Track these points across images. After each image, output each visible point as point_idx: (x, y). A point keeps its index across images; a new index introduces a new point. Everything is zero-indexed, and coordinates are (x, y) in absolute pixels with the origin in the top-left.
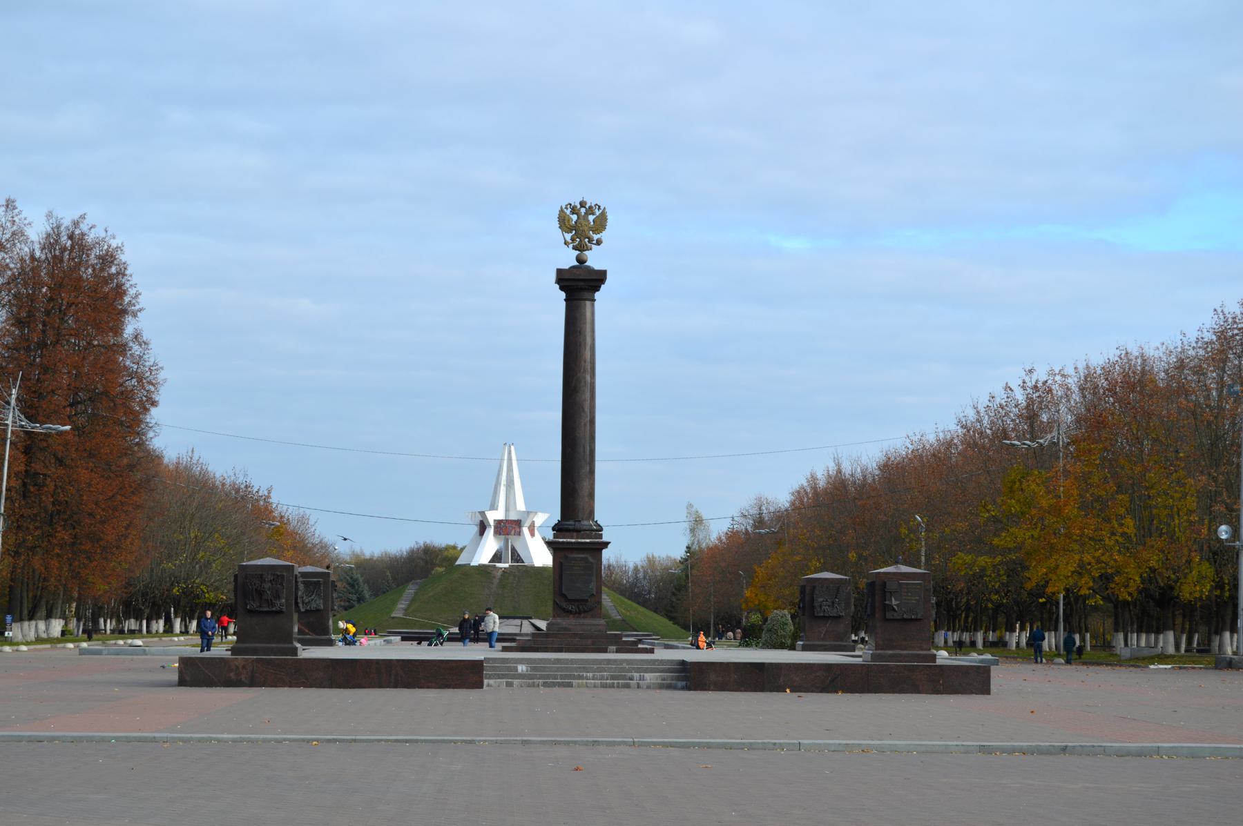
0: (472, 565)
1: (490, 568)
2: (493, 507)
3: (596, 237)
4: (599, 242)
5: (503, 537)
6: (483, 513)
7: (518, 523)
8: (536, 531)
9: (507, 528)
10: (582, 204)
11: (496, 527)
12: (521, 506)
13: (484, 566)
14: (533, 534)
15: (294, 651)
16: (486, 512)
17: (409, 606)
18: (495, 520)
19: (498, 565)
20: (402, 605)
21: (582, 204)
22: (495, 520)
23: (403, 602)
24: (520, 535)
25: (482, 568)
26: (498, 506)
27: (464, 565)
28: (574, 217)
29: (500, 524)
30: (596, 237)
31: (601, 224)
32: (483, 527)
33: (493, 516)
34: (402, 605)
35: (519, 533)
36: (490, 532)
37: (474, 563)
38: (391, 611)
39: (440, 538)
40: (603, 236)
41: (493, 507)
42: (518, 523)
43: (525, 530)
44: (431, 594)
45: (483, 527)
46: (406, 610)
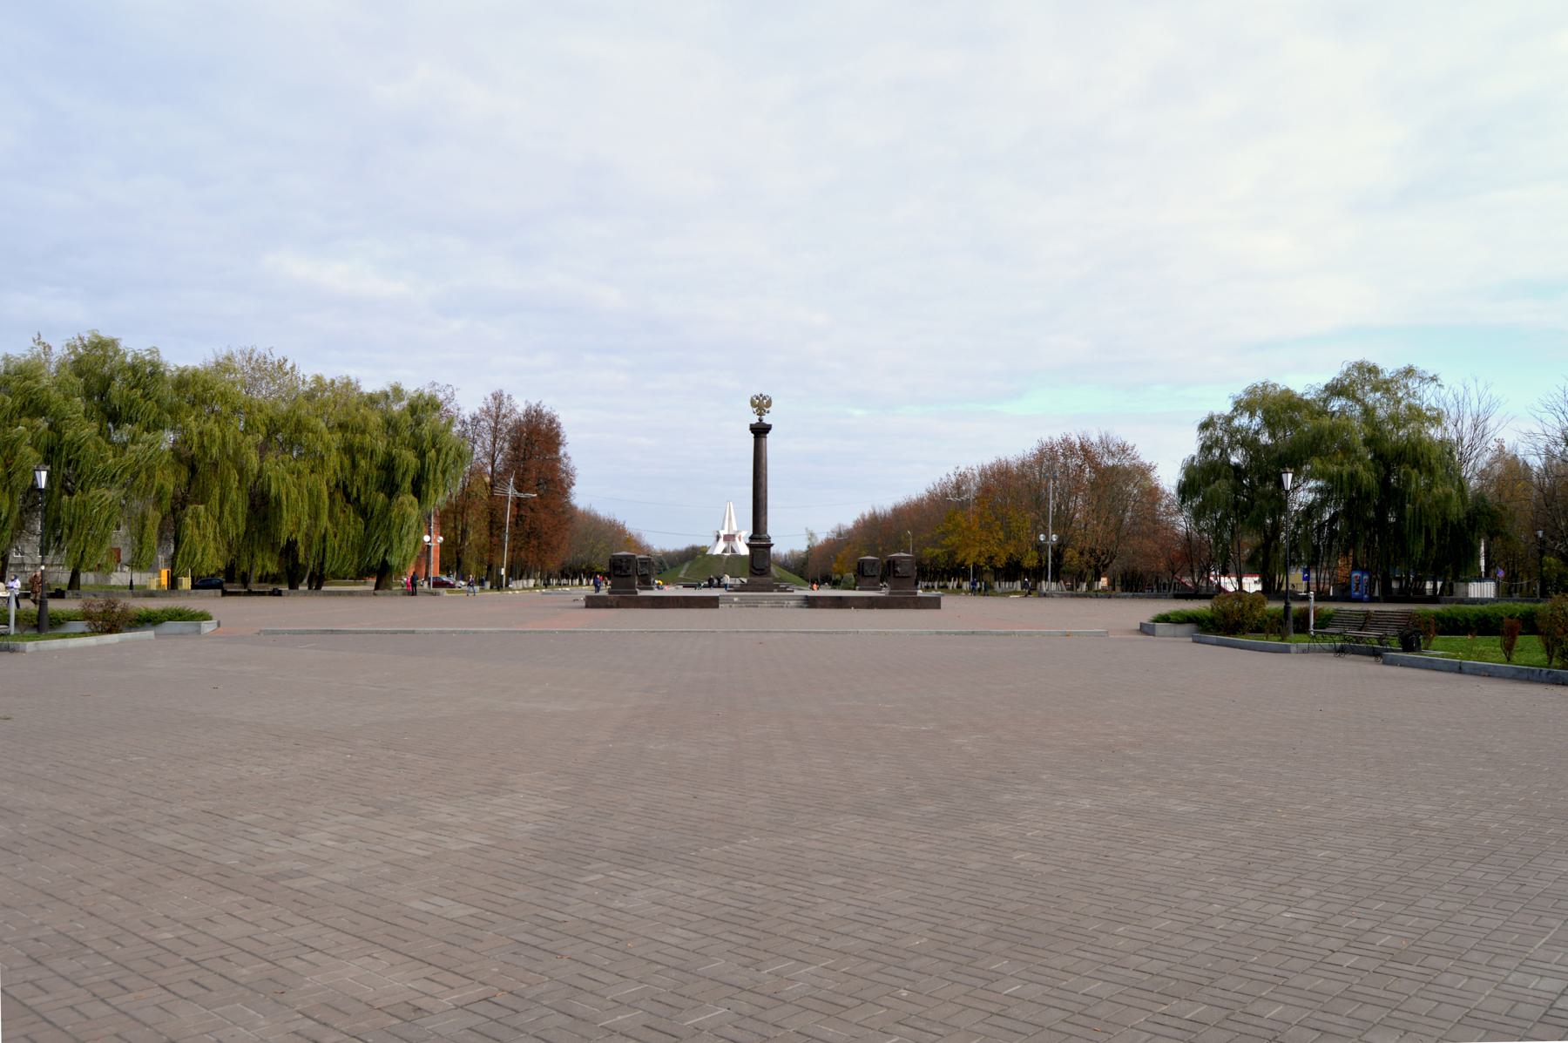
2: (723, 529)
3: (767, 410)
4: (768, 412)
6: (718, 532)
7: (734, 536)
9: (729, 538)
10: (761, 395)
12: (735, 528)
13: (718, 555)
15: (636, 593)
21: (761, 395)
25: (718, 556)
28: (758, 401)
30: (767, 410)
31: (769, 404)
32: (718, 538)
33: (722, 533)
35: (734, 540)
36: (721, 540)
37: (715, 553)
39: (699, 543)
40: (770, 409)
41: (723, 529)
42: (734, 536)
43: (737, 539)
45: (718, 538)
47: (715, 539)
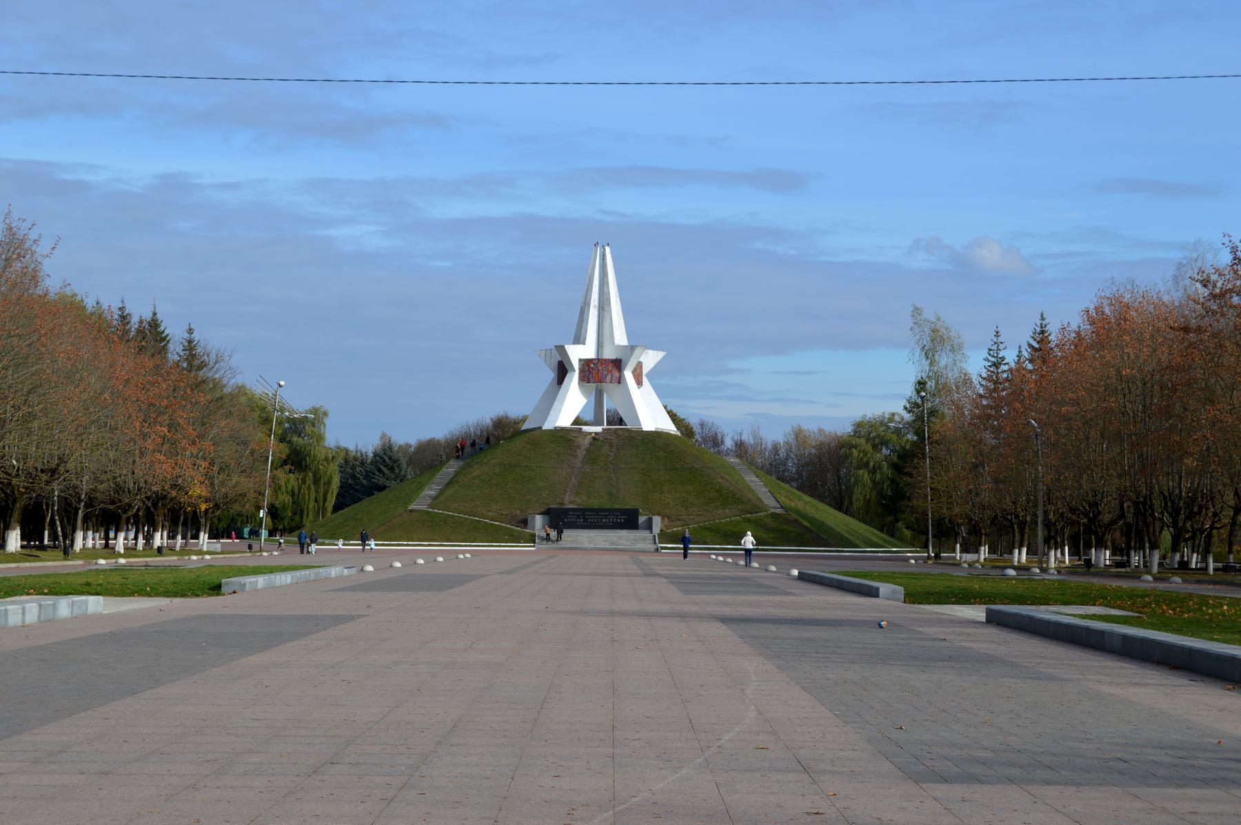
0: (544, 428)
1: (571, 433)
2: (579, 339)
5: (593, 386)
6: (561, 349)
7: (618, 364)
8: (645, 380)
11: (582, 371)
13: (563, 429)
14: (639, 383)
16: (566, 347)
17: (441, 492)
18: (580, 360)
19: (585, 428)
20: (430, 491)
22: (580, 360)
23: (434, 486)
24: (619, 382)
25: (560, 432)
26: (585, 338)
27: (534, 429)
29: (589, 366)
32: (562, 370)
33: (578, 354)
34: (430, 491)
36: (573, 380)
37: (547, 426)
38: (410, 501)
41: (579, 339)
42: (618, 364)
43: (628, 374)
44: (477, 473)
46: (435, 498)
47: (551, 375)
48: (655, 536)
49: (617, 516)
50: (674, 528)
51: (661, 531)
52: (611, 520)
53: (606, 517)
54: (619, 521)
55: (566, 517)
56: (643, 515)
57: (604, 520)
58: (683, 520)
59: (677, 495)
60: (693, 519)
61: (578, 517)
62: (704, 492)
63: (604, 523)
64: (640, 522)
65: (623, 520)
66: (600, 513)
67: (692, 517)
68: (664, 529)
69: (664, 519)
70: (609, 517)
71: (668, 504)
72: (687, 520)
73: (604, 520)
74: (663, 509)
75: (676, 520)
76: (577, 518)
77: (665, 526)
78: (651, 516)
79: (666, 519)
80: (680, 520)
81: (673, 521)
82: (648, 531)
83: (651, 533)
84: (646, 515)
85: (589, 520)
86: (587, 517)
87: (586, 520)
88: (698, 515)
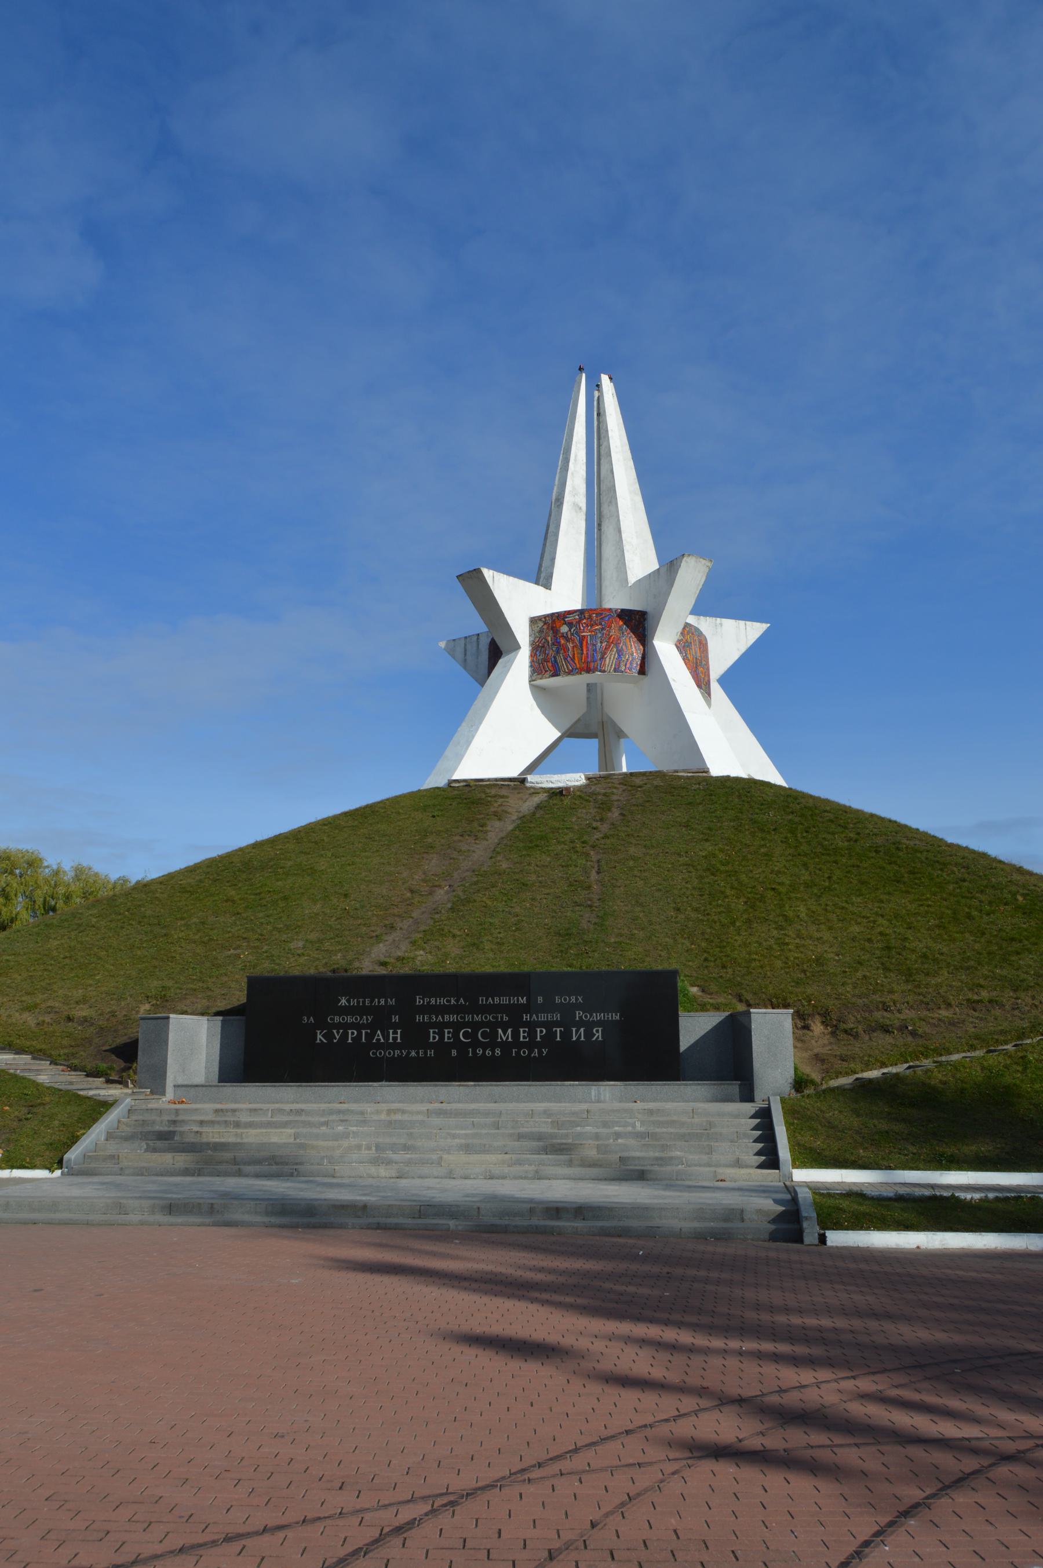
48: (765, 1115)
49: (568, 1011)
50: (868, 1067)
51: (800, 1084)
52: (540, 1032)
53: (515, 1023)
54: (578, 1034)
55: (321, 1024)
56: (703, 1008)
57: (505, 1036)
58: (903, 1028)
59: (855, 929)
60: (952, 1023)
61: (381, 1020)
62: (969, 917)
63: (505, 1046)
64: (687, 1039)
65: (598, 1034)
66: (482, 1000)
67: (944, 1013)
68: (816, 1076)
69: (806, 1027)
70: (526, 1017)
71: (819, 961)
72: (923, 1028)
73: (505, 1036)
74: (798, 983)
75: (871, 1030)
76: (373, 1027)
77: (818, 1058)
78: (741, 1007)
79: (817, 1027)
80: (886, 1030)
81: (856, 1036)
82: (734, 1087)
83: (748, 1096)
84: (717, 1008)
85: (433, 1036)
86: (419, 1018)
87: (415, 1035)
88: (973, 1004)
